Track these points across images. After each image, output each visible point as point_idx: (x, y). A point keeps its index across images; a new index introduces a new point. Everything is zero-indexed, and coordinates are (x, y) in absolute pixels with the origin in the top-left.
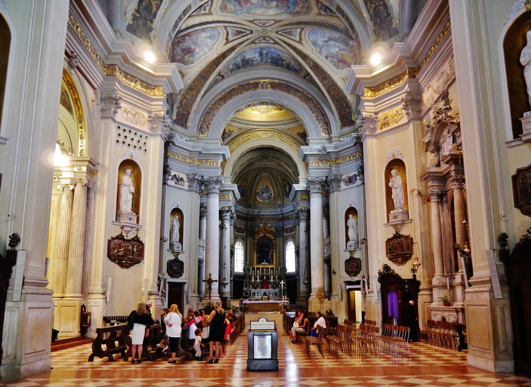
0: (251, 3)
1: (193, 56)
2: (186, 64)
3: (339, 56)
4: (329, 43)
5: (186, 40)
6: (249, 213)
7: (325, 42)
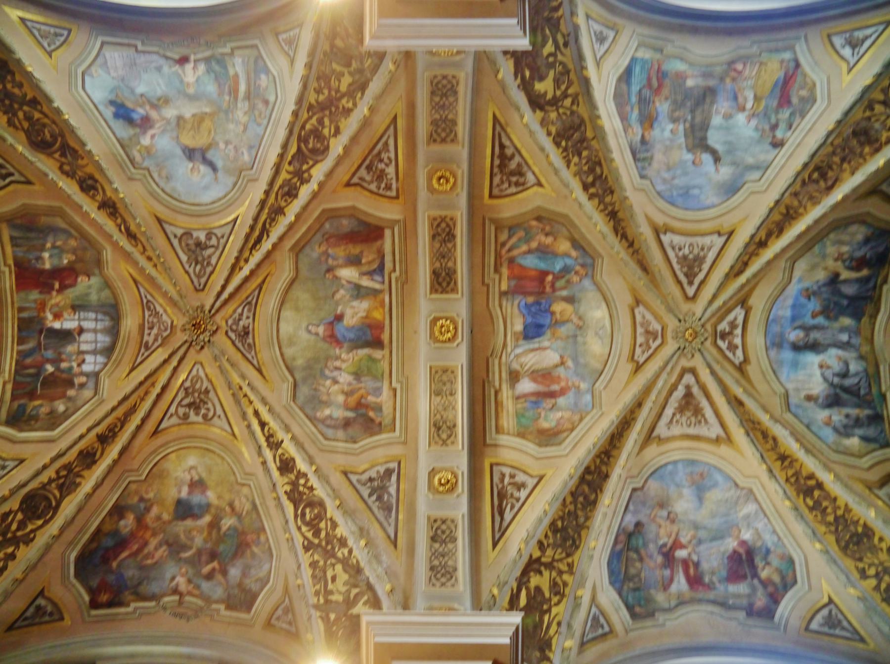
0: (556, 366)
1: (768, 551)
2: (789, 579)
3: (766, 107)
4: (719, 147)
5: (695, 558)
7: (717, 159)
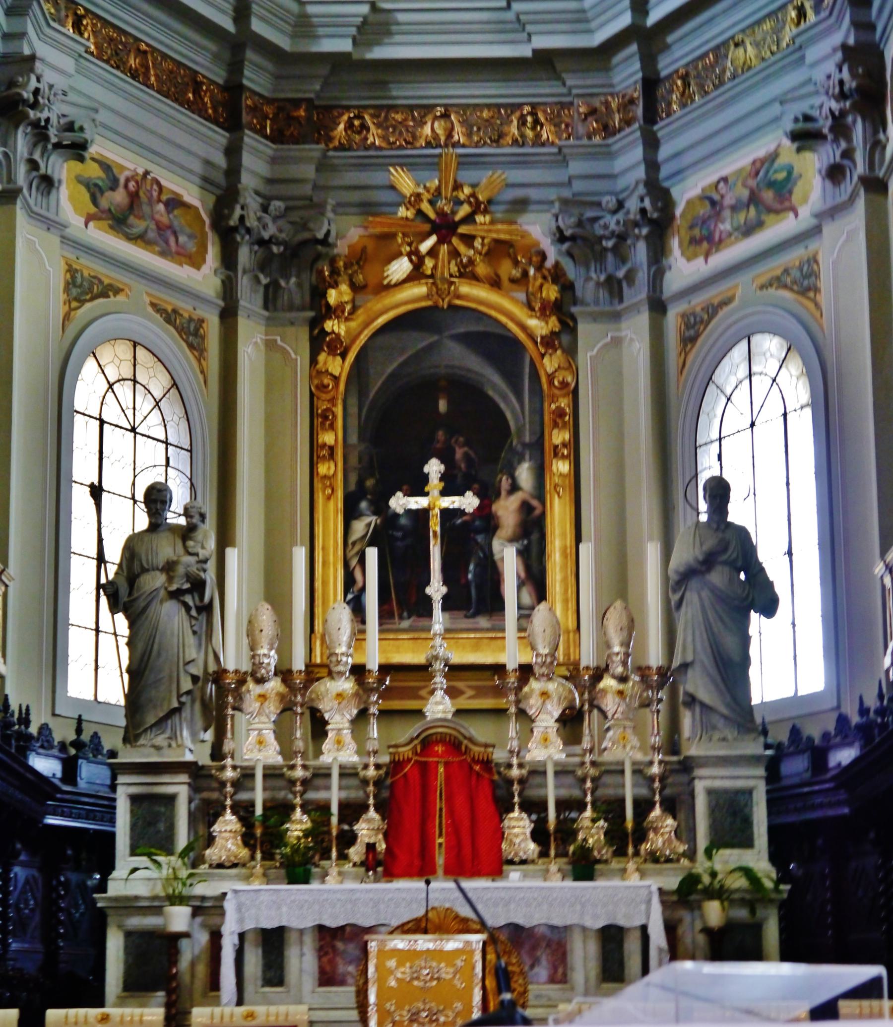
6: (257, 26)
